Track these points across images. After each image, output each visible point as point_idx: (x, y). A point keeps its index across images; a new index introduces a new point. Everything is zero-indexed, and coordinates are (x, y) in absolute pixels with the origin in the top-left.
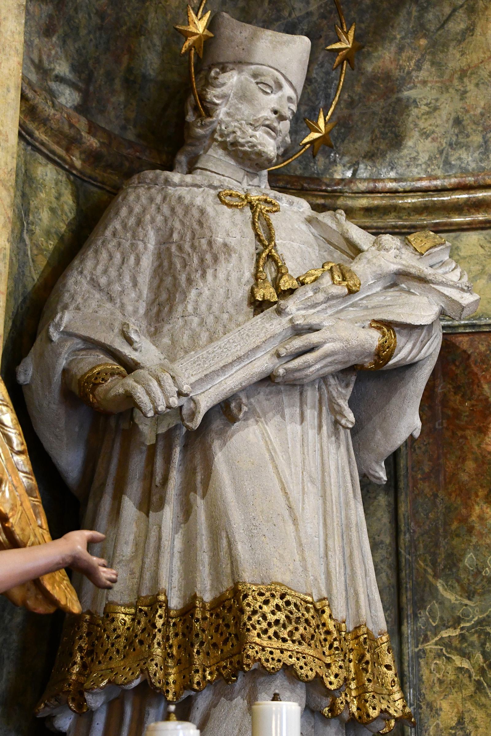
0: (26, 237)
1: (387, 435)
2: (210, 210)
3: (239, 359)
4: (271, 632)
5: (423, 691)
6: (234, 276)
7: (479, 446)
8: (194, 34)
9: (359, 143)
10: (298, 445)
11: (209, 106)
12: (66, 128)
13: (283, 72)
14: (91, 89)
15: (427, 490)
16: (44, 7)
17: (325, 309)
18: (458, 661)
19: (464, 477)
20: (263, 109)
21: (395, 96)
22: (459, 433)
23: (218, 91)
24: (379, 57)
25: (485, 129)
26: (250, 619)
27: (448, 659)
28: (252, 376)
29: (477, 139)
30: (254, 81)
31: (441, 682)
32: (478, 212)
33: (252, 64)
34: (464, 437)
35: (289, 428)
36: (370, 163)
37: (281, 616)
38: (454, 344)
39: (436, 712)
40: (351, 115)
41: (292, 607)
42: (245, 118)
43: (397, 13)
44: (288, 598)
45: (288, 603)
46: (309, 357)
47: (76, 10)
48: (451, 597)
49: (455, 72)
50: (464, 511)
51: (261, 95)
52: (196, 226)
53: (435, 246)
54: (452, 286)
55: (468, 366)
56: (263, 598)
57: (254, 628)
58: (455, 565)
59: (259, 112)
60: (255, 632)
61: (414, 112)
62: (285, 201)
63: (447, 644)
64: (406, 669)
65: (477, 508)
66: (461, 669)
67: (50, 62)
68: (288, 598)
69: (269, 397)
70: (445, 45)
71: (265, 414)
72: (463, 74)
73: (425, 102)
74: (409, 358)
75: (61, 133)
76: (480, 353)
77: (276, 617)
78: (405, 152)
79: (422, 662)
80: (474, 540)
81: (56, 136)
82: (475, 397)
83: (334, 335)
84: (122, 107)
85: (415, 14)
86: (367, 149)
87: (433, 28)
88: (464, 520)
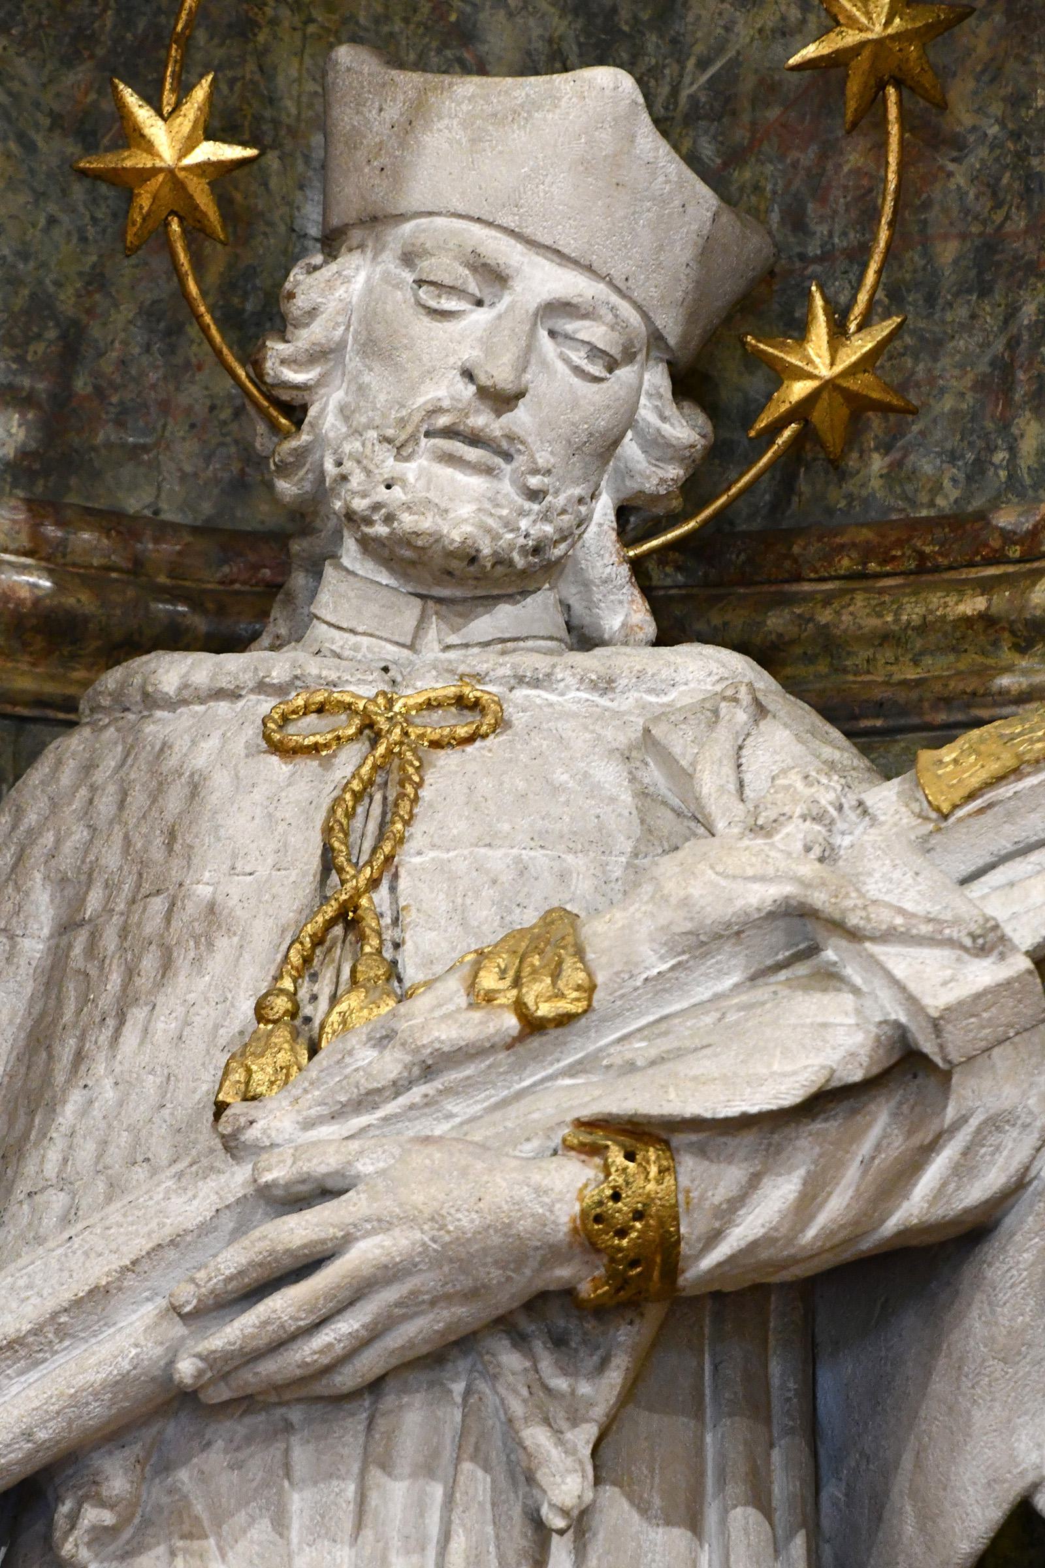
1: (926, 1519)
6: (204, 1017)
11: (285, 396)
13: (510, 221)
14: (82, 384)
17: (429, 1102)
20: (430, 373)
28: (75, 1401)
30: (409, 277)
33: (402, 218)
42: (378, 421)
52: (157, 853)
53: (1015, 773)
59: (414, 389)
62: (572, 681)
69: (241, 1456)
71: (218, 1521)
74: (811, 1233)
83: (388, 1205)
84: (226, 414)
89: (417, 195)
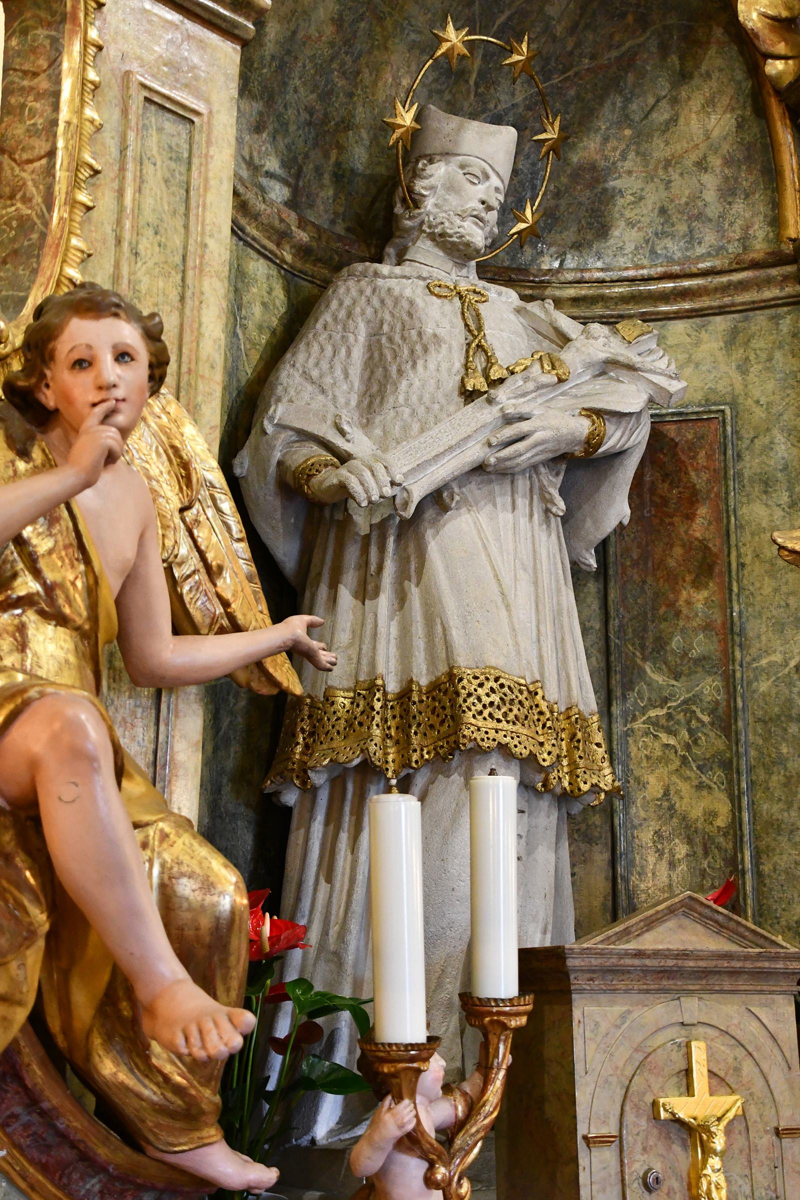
0: (239, 331)
1: (596, 522)
2: (419, 302)
3: (451, 449)
4: (486, 713)
5: (631, 767)
6: (444, 366)
7: (686, 532)
8: (401, 126)
9: (566, 233)
10: (510, 533)
11: (417, 197)
12: (277, 223)
14: (301, 184)
15: (636, 577)
16: (254, 104)
17: (535, 398)
18: (665, 738)
19: (672, 563)
21: (601, 186)
22: (667, 520)
23: (425, 183)
24: (585, 148)
25: (690, 218)
26: (465, 701)
27: (656, 736)
29: (682, 228)
30: (461, 172)
31: (648, 758)
32: (684, 301)
34: (672, 524)
35: (501, 516)
36: (577, 253)
37: (495, 698)
38: (661, 433)
39: (642, 785)
40: (557, 206)
41: (506, 689)
43: (601, 104)
44: (502, 681)
45: (502, 686)
46: (520, 446)
47: (285, 107)
48: (659, 678)
49: (659, 161)
50: (671, 596)
51: (469, 185)
52: (406, 318)
53: (643, 334)
54: (661, 374)
55: (675, 454)
56: (478, 681)
57: (470, 710)
58: (662, 648)
60: (470, 714)
61: (620, 201)
63: (654, 723)
64: (615, 747)
65: (684, 592)
66: (667, 745)
67: (260, 159)
68: (502, 681)
70: (650, 136)
72: (667, 164)
73: (630, 192)
75: (272, 227)
76: (687, 442)
77: (490, 699)
78: (612, 241)
79: (630, 740)
80: (681, 623)
81: (266, 231)
82: (682, 484)
83: (545, 423)
85: (619, 104)
86: (574, 240)
87: (637, 119)
88: (671, 605)
89: (464, 149)
